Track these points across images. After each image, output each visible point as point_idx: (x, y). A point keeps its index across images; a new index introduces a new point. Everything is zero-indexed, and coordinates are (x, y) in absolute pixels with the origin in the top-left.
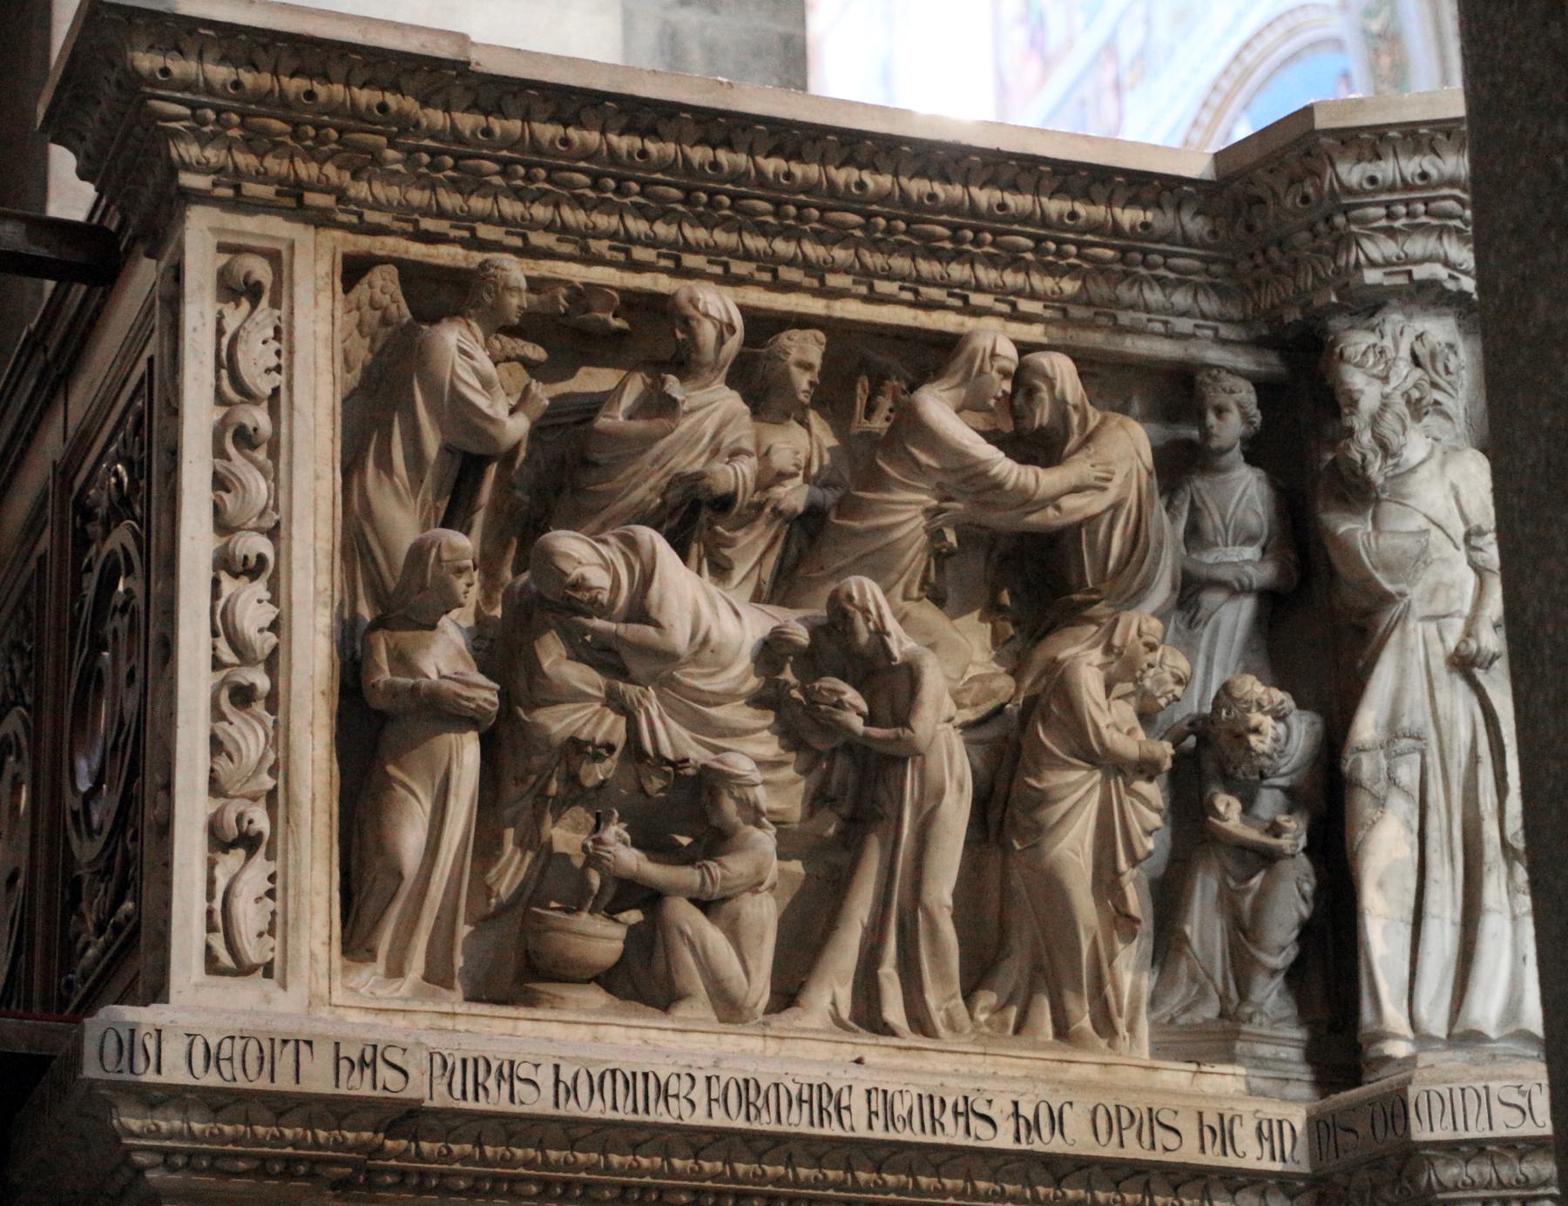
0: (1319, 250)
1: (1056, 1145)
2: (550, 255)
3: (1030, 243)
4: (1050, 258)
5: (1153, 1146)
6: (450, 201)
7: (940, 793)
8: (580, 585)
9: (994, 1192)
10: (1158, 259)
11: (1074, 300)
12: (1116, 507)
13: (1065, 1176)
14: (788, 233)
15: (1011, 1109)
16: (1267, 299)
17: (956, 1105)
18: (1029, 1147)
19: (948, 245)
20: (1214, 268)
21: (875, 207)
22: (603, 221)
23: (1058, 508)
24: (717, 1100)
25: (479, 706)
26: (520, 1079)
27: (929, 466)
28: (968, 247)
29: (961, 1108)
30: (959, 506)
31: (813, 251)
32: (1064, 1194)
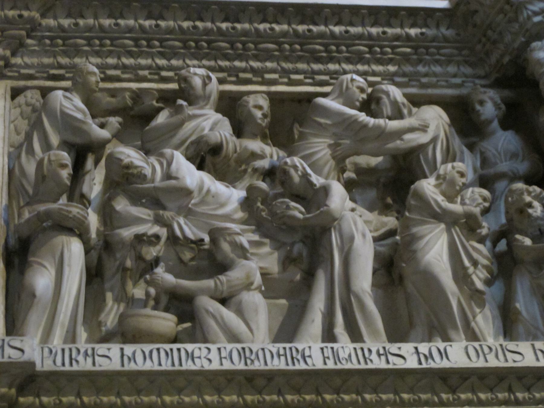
0: (510, 21)
1: (445, 364)
2: (119, 79)
3: (366, 49)
4: (379, 56)
5: (506, 360)
6: (64, 61)
7: (352, 239)
8: (128, 167)
9: (414, 400)
10: (432, 50)
11: (395, 74)
12: (434, 140)
13: (457, 388)
14: (240, 58)
15: (414, 350)
16: (493, 59)
17: (378, 351)
18: (428, 366)
19: (324, 54)
20: (465, 52)
21: (282, 40)
22: (143, 62)
23: (402, 140)
24: (225, 358)
25: (75, 216)
26: (99, 356)
27: (326, 124)
28: (335, 54)
29: (382, 352)
30: (347, 142)
31: (255, 64)
32: (459, 397)
